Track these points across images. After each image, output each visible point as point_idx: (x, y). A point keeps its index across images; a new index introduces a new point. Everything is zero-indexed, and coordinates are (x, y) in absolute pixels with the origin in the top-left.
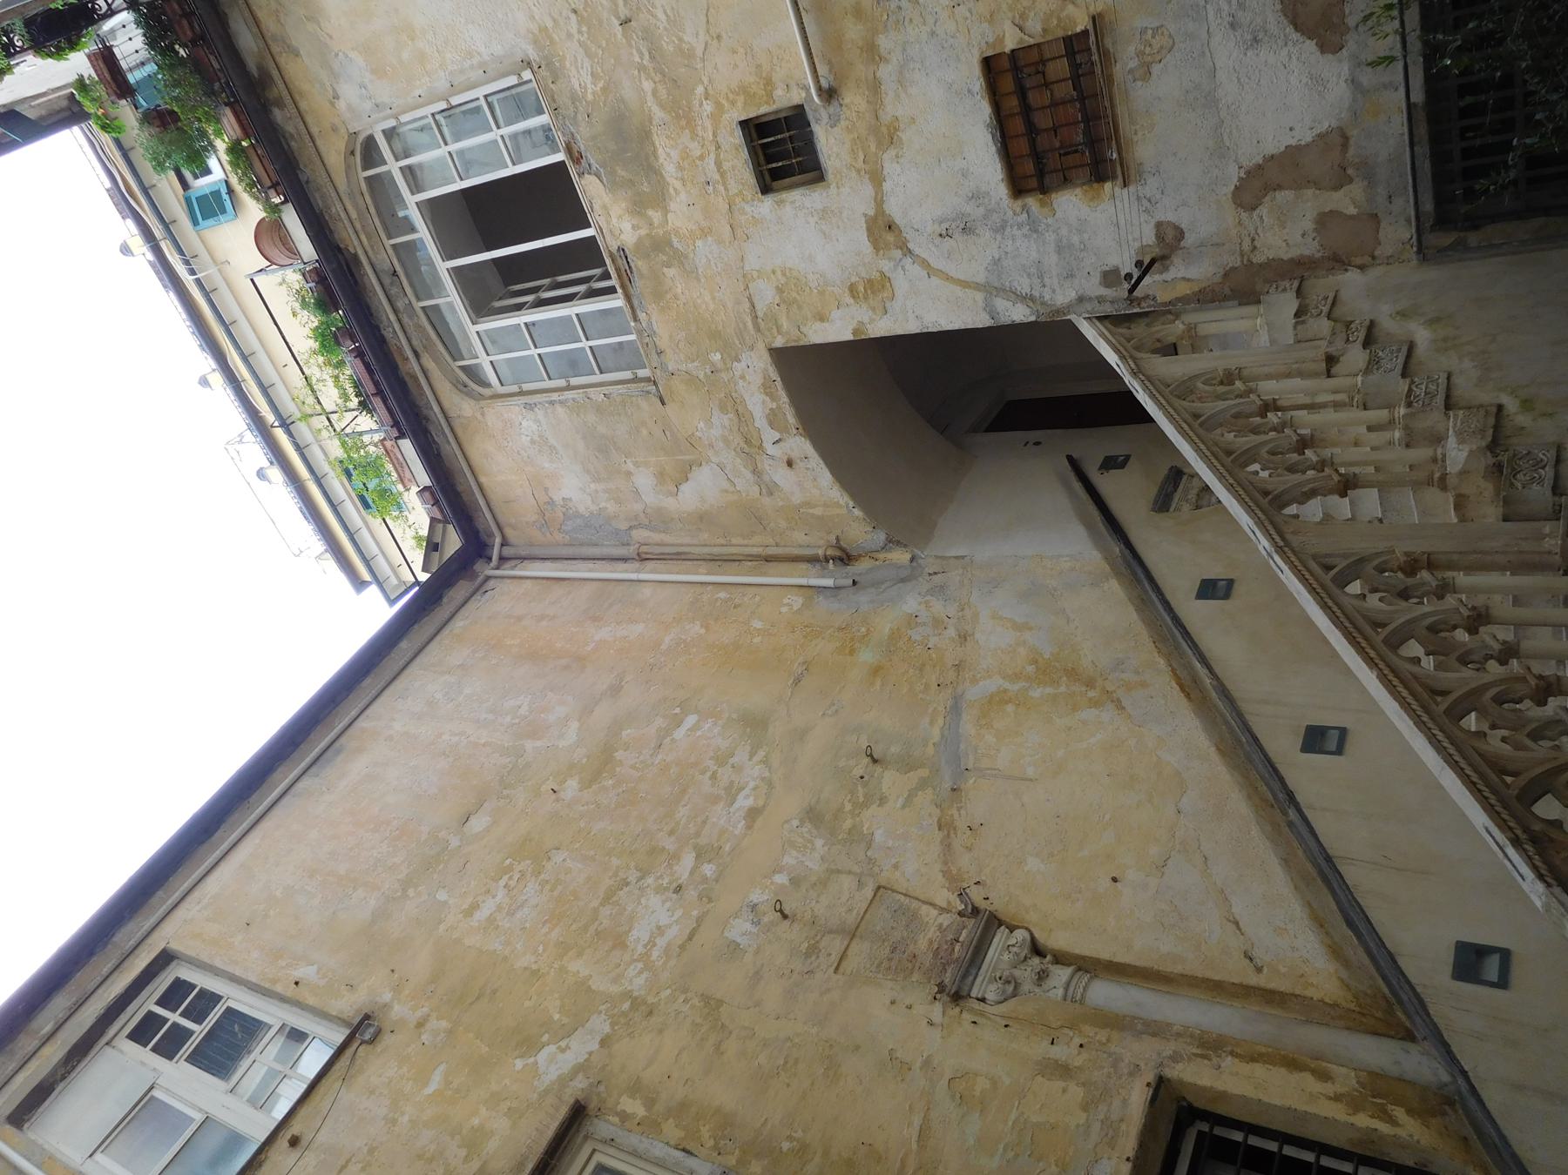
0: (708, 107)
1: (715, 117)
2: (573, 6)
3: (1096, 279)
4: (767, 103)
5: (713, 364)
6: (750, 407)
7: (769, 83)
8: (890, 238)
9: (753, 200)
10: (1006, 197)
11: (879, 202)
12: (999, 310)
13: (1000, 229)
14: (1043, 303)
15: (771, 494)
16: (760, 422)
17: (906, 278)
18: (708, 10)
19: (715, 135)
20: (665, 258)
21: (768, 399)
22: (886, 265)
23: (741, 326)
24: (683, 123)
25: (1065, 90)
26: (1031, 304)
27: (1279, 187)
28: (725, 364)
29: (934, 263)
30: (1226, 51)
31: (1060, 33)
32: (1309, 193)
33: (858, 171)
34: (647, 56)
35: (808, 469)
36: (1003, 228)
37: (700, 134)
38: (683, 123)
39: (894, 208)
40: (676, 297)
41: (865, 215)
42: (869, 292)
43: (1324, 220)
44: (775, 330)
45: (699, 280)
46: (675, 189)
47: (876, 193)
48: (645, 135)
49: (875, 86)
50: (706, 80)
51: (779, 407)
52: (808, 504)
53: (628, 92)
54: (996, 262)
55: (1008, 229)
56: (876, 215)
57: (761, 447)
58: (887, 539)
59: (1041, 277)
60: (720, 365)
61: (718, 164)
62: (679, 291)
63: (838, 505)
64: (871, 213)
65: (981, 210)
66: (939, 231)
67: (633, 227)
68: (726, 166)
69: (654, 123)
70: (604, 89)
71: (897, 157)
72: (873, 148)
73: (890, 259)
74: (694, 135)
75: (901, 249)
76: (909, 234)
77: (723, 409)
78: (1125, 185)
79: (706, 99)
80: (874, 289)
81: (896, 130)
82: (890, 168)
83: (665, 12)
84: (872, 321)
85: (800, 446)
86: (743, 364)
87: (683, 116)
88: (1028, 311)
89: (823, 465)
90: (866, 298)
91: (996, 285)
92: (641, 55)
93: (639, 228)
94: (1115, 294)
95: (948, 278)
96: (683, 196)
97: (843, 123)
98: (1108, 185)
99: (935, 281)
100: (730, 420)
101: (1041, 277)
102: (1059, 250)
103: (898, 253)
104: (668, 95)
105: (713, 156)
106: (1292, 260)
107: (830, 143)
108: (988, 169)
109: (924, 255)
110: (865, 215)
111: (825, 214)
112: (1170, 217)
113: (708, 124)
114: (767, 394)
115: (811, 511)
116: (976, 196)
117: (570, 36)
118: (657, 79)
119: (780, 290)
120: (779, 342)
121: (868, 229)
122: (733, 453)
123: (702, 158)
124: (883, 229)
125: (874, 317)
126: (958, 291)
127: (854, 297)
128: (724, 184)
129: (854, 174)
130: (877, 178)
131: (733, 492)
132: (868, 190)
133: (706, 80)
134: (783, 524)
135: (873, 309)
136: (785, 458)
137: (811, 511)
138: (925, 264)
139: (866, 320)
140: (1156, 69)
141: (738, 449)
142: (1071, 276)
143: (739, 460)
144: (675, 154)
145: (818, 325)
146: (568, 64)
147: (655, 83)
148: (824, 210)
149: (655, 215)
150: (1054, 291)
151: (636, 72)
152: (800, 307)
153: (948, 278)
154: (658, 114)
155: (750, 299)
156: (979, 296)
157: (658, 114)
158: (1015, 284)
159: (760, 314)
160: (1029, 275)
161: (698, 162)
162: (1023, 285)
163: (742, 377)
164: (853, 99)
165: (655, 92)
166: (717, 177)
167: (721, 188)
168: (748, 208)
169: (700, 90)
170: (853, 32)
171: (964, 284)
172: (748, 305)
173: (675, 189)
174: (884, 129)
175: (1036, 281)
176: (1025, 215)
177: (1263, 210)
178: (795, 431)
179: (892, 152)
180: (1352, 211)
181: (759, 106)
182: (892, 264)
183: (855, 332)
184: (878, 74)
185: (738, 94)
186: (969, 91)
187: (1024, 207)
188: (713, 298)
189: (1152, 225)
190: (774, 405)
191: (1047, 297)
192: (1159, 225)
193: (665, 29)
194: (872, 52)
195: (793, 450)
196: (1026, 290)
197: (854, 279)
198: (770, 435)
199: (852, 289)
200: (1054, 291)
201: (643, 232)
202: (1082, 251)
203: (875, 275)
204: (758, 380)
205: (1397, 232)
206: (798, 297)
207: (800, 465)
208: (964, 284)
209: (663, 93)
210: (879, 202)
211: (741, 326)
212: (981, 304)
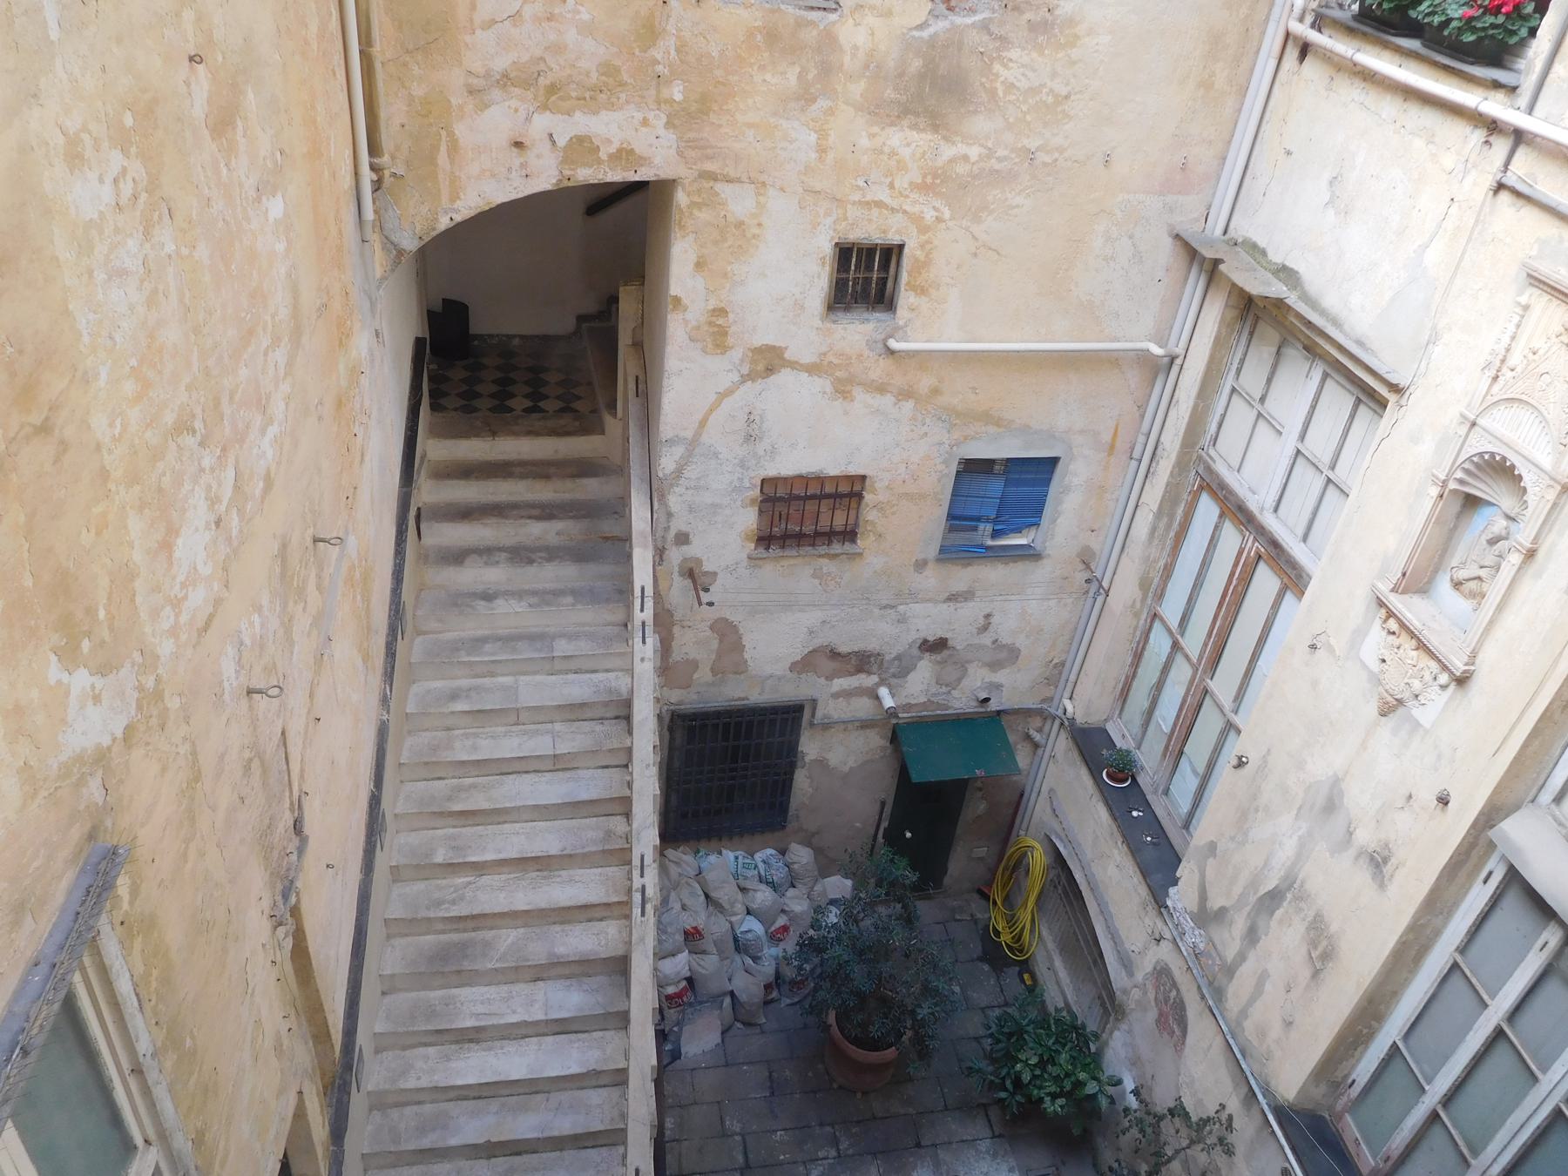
0: (929, 215)
1: (917, 220)
2: (1072, 98)
3: (684, 528)
4: (908, 283)
5: (669, 82)
6: (605, 116)
7: (922, 291)
8: (760, 367)
9: (835, 230)
10: (766, 473)
11: (794, 365)
12: (673, 448)
13: (742, 464)
14: (672, 485)
15: (471, 91)
16: (583, 123)
17: (723, 369)
18: (998, 254)
19: (905, 212)
20: (810, 77)
21: (612, 149)
22: (736, 354)
23: (709, 151)
24: (929, 180)
25: (824, 523)
26: (673, 476)
27: (721, 641)
28: (666, 101)
29: (727, 404)
30: (812, 618)
31: (859, 531)
32: (714, 657)
33: (825, 354)
34: (997, 167)
35: (510, 169)
36: (742, 467)
37: (912, 196)
38: (929, 180)
39: (785, 377)
40: (762, 68)
41: (786, 348)
42: (716, 329)
43: (694, 665)
44: (696, 199)
45: (775, 114)
46: (874, 135)
47: (801, 365)
48: (937, 124)
49: (881, 389)
50: (950, 224)
51: (599, 162)
52: (454, 148)
53: (981, 124)
54: (716, 455)
55: (741, 470)
56: (784, 359)
57: (544, 107)
58: (405, 251)
59: (696, 488)
60: (665, 93)
61: (879, 204)
62: (768, 77)
63: (454, 197)
64: (787, 355)
65: (761, 453)
66: (754, 412)
67: (856, 48)
68: (875, 212)
69: (942, 143)
70: (993, 93)
71: (824, 393)
72: (838, 374)
73: (742, 361)
74: (914, 186)
75: (748, 375)
76: (759, 385)
77: (608, 70)
78: (750, 558)
79: (937, 218)
80: (717, 334)
81: (845, 398)
82: (822, 384)
83: (1017, 206)
84: (686, 322)
85: (544, 177)
86: (661, 131)
87: (934, 182)
88: (667, 472)
89: (514, 196)
90: (710, 324)
91: (696, 450)
92: (1000, 160)
93: (854, 56)
94: (669, 540)
95: (711, 411)
96: (864, 142)
97: (866, 353)
98: (752, 546)
99: (713, 397)
100: (588, 74)
101: (696, 488)
102: (714, 506)
103: (745, 370)
104: (957, 174)
105: (888, 201)
106: (670, 646)
107: (858, 330)
108: (791, 463)
109: (737, 393)
110: (786, 348)
111: (799, 306)
112: (719, 581)
113: (917, 209)
114: (620, 151)
115: (443, 148)
116: (773, 452)
117: (1054, 75)
118: (975, 168)
119: (740, 225)
120: (681, 198)
121: (774, 347)
122: (538, 53)
123: (891, 186)
124: (769, 361)
125: (690, 326)
126: (699, 416)
127: (714, 310)
128: (860, 202)
129: (824, 349)
130: (813, 369)
131: (471, 20)
132: (807, 358)
133: (950, 224)
134: (418, 91)
135: (698, 328)
136: (527, 143)
137: (443, 148)
138: (729, 392)
139: (689, 316)
140: (817, 582)
141: (542, 66)
142: (691, 510)
143: (525, 58)
144: (906, 153)
145: (693, 258)
146: (1034, 55)
147: (973, 164)
148: (802, 307)
149: (857, 89)
150: (681, 495)
151: (990, 145)
152: (716, 243)
153: (711, 411)
154: (948, 152)
155: (739, 180)
156: (689, 434)
157: (948, 152)
158: (694, 467)
159: (719, 187)
160: (699, 479)
161: (890, 179)
162: (691, 472)
163: (645, 122)
164: (879, 369)
165: (966, 158)
166: (868, 198)
167: (856, 197)
168: (829, 221)
169: (947, 214)
170: (925, 382)
171: (703, 423)
172: (732, 174)
173: (874, 135)
174: (848, 388)
175: (693, 484)
176: (748, 485)
177: (709, 633)
178: (567, 173)
179: (829, 389)
180: (695, 676)
181: (910, 275)
182: (737, 362)
183: (677, 300)
184: (889, 395)
185: (927, 256)
186: (850, 463)
187: (755, 486)
188: (750, 125)
189: (717, 570)
190: (603, 155)
191: (677, 489)
192: (715, 574)
193: (1006, 199)
194: (905, 394)
195: (539, 156)
196: (686, 474)
197: (731, 316)
198: (566, 127)
199: (721, 312)
200: (681, 495)
201: (847, 59)
202: (710, 522)
203: (730, 341)
204: (641, 143)
205: (675, 696)
206: (726, 245)
207: (515, 159)
208: (703, 423)
209: (961, 169)
210: (794, 365)
211: (709, 151)
212: (683, 434)
